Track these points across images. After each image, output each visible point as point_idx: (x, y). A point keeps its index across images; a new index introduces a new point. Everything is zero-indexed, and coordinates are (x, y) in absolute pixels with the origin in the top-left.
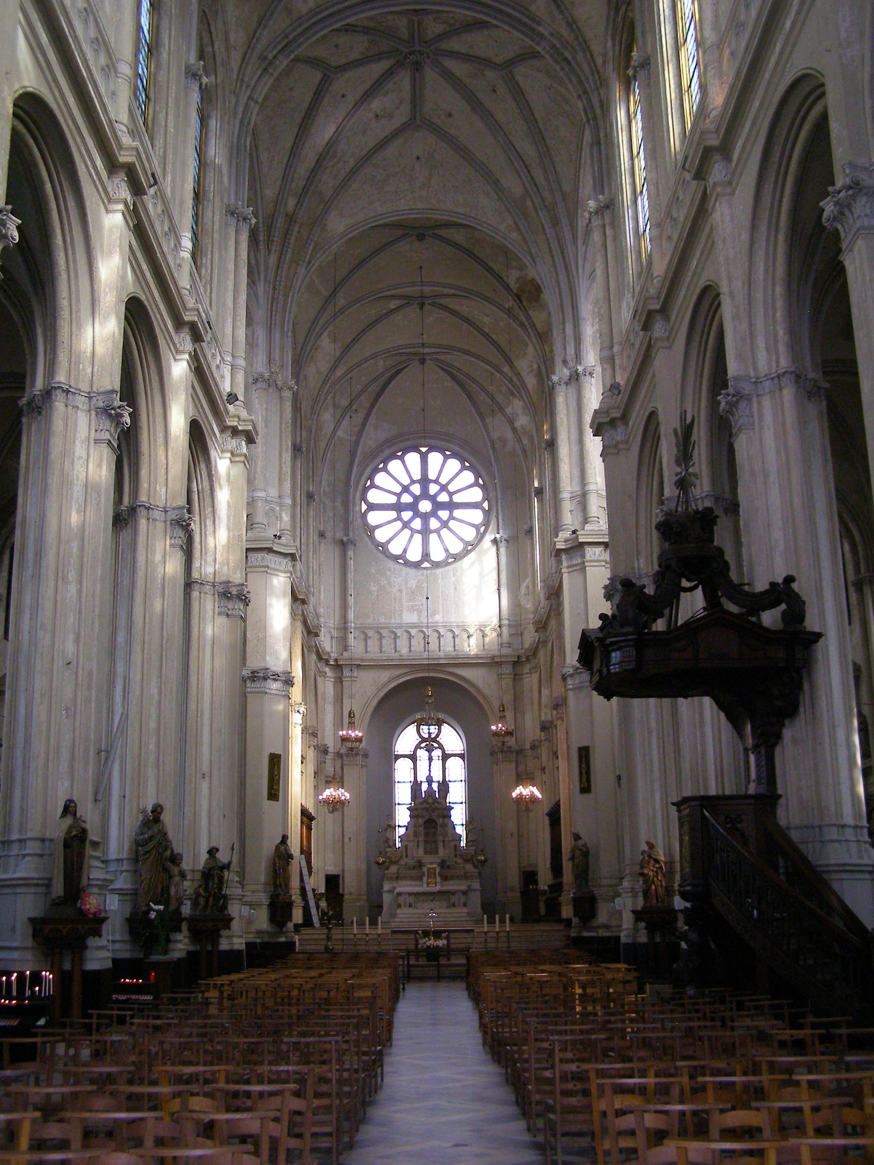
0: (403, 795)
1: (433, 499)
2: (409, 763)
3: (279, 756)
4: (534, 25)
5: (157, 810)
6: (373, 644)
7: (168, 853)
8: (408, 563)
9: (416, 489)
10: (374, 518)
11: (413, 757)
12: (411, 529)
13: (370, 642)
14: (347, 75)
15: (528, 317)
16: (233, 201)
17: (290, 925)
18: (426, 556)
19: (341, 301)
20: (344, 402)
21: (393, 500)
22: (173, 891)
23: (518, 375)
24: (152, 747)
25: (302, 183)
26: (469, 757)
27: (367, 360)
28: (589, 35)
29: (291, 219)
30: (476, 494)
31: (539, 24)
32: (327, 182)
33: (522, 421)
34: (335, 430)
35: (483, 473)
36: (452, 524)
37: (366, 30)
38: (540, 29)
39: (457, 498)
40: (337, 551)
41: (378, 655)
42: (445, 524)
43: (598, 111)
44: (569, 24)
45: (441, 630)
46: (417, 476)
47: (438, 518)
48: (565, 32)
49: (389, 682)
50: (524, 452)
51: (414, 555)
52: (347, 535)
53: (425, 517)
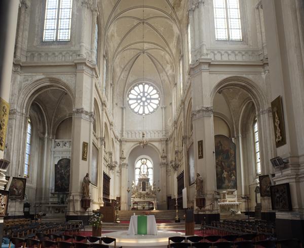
0: (137, 177)
2: (139, 170)
3: (87, 144)
6: (130, 135)
8: (139, 114)
9: (142, 94)
10: (131, 102)
11: (140, 168)
13: (129, 135)
15: (176, 16)
18: (144, 112)
21: (135, 97)
23: (170, 50)
26: (154, 169)
30: (157, 96)
33: (170, 72)
36: (151, 104)
40: (121, 110)
41: (131, 138)
42: (149, 104)
45: (148, 132)
46: (142, 91)
49: (134, 145)
50: (170, 82)
51: (141, 112)
52: (123, 105)
53: (144, 102)
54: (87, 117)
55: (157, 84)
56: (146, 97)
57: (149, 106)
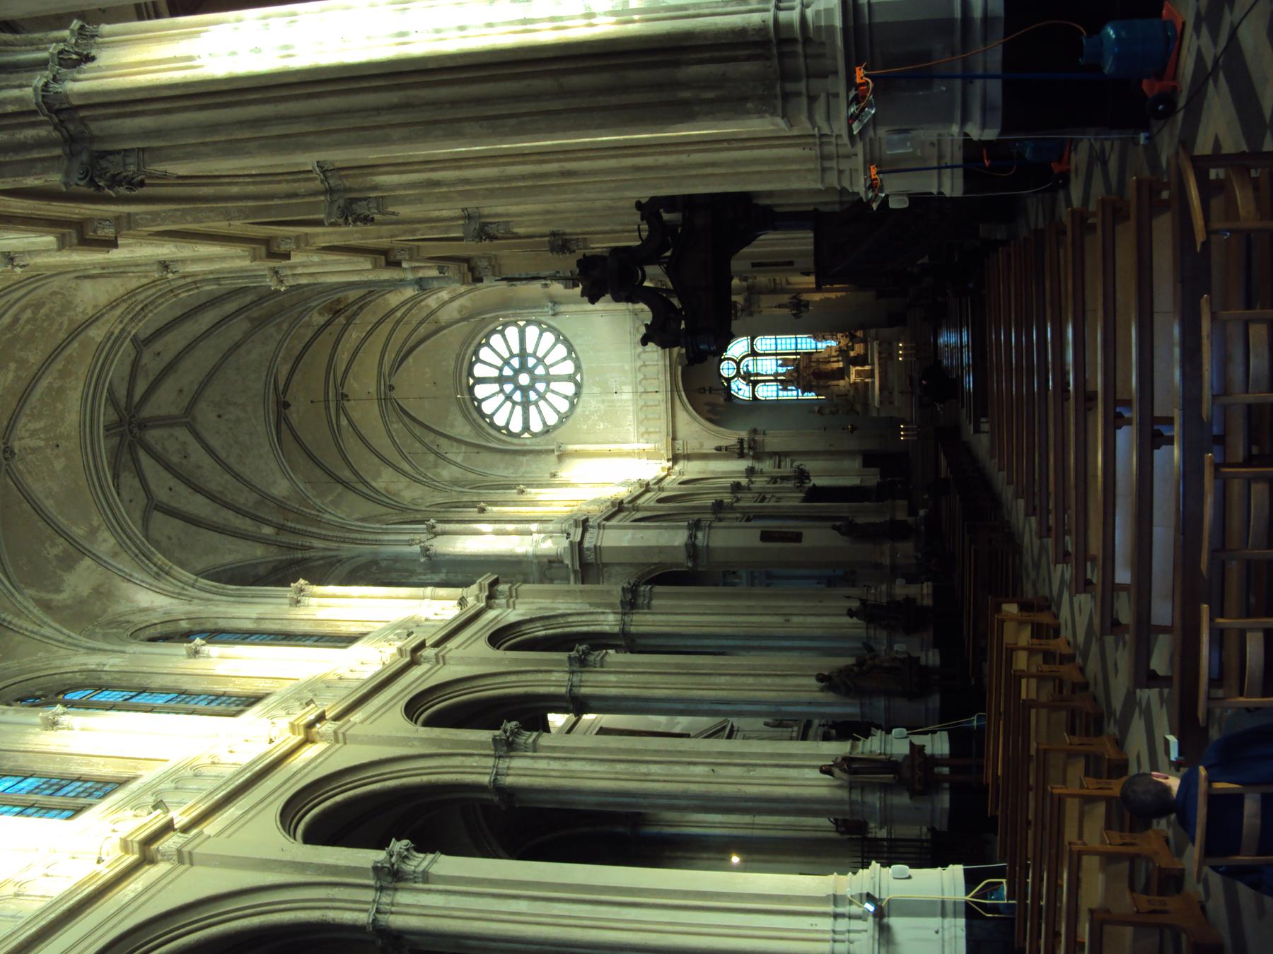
1: (517, 372)
2: (760, 387)
4: (113, 338)
5: (820, 678)
7: (855, 669)
8: (577, 394)
9: (508, 388)
10: (536, 426)
12: (546, 392)
14: (152, 486)
16: (287, 601)
17: (911, 520)
18: (570, 378)
19: (346, 474)
20: (432, 457)
21: (519, 409)
22: (886, 664)
23: (404, 303)
24: (769, 681)
25: (248, 521)
27: (394, 442)
28: (122, 291)
29: (280, 528)
30: (512, 332)
31: (112, 333)
32: (245, 498)
34: (455, 464)
35: (491, 327)
36: (540, 354)
37: (116, 476)
38: (117, 332)
39: (516, 350)
42: (540, 361)
43: (189, 280)
44: (113, 308)
46: (496, 387)
47: (535, 367)
48: (118, 312)
49: (687, 411)
51: (570, 389)
52: (553, 451)
54: (700, 535)
55: (472, 335)
56: (517, 372)
57: (548, 361)
